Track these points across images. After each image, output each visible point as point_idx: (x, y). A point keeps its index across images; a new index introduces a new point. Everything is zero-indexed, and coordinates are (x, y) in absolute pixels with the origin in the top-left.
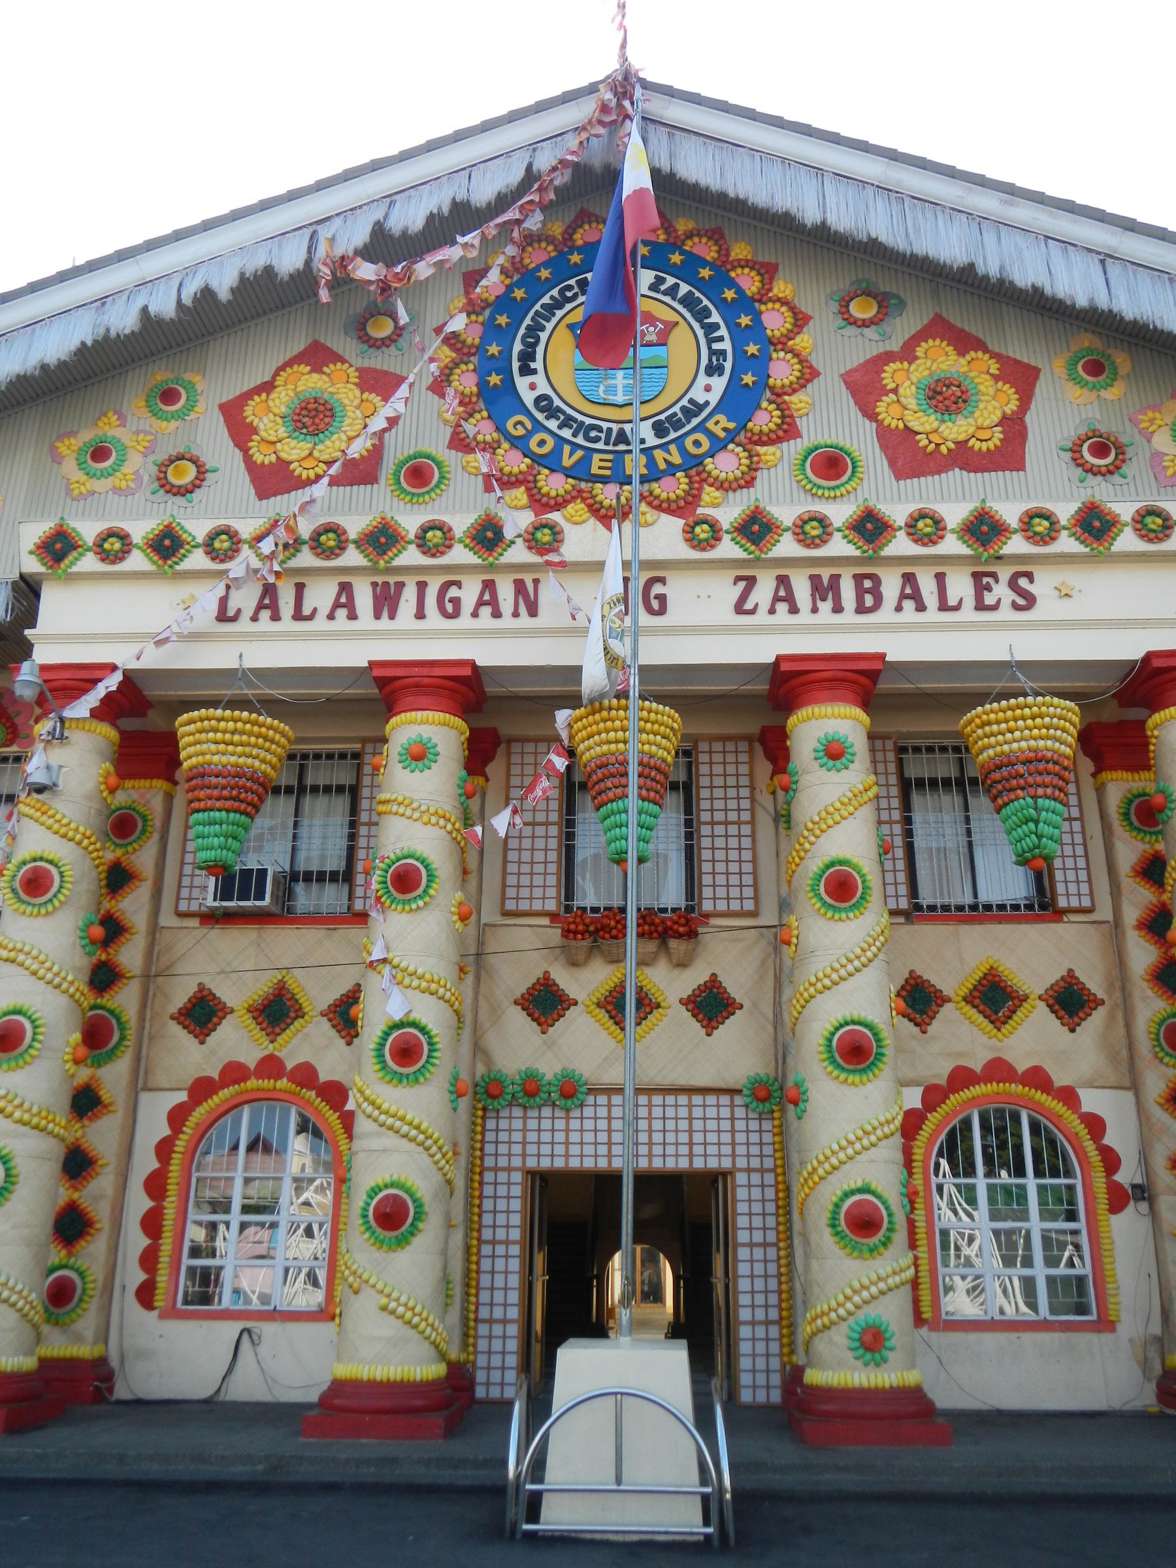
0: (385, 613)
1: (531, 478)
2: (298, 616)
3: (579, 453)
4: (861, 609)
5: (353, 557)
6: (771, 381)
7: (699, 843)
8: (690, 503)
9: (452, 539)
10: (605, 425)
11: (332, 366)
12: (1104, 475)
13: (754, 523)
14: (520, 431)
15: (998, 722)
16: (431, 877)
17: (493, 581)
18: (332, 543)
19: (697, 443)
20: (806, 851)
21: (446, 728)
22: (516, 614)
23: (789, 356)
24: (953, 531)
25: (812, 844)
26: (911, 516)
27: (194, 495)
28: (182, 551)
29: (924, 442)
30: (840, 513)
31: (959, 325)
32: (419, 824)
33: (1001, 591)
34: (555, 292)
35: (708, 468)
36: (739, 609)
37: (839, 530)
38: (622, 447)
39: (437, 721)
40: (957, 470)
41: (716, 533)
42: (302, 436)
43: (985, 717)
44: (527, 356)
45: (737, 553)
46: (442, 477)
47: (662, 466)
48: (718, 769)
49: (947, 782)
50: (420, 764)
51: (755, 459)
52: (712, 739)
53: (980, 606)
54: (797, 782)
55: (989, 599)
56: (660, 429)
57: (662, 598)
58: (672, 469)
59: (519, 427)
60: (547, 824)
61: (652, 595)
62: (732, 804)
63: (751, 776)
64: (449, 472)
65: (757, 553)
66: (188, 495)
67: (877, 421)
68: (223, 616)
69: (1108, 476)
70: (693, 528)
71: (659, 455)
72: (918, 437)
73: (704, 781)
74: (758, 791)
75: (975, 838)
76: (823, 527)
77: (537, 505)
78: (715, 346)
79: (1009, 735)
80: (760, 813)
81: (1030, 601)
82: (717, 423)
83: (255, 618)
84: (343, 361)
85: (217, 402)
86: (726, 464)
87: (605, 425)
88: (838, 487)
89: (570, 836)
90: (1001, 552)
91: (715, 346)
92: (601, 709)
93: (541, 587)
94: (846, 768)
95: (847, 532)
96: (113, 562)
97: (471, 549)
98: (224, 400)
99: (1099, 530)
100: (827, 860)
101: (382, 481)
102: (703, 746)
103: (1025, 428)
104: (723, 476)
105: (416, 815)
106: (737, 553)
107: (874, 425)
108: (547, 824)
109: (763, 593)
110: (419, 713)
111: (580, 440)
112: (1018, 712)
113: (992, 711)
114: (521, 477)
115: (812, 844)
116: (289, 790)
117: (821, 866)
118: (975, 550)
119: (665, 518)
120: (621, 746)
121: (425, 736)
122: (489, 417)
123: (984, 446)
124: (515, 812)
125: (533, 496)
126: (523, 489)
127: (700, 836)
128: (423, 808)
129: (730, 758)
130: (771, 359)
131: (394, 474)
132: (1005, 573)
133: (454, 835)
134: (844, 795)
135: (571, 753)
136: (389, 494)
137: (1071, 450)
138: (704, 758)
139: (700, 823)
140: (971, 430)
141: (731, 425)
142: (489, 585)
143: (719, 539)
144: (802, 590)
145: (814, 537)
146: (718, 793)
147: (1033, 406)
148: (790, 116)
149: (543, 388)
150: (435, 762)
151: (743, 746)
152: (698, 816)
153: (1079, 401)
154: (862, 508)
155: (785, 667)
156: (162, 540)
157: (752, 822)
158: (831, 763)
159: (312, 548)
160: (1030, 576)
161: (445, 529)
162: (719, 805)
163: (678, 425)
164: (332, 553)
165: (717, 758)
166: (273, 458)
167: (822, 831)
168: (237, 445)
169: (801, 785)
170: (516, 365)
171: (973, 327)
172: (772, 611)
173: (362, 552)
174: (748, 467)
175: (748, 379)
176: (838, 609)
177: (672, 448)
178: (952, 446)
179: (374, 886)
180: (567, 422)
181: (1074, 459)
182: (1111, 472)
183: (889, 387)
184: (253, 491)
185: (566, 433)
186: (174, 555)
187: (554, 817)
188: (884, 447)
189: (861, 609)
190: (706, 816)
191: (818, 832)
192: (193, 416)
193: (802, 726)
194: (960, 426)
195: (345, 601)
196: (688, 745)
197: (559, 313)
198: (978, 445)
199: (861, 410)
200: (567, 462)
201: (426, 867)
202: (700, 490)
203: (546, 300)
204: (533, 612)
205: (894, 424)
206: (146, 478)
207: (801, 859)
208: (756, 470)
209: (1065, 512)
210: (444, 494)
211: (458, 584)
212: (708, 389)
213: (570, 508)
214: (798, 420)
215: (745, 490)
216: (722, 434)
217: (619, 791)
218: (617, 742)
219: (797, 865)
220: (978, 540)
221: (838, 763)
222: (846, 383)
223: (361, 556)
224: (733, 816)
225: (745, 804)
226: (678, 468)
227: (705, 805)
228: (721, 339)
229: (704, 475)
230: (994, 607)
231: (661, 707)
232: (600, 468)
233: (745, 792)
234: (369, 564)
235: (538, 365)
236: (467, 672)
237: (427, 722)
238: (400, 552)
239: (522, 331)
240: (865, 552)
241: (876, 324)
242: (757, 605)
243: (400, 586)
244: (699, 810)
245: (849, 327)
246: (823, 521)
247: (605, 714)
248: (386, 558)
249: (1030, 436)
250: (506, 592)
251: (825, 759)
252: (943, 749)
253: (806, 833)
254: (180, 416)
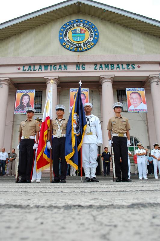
10: (76, 44)
14: (65, 45)
19: (89, 46)
34: (69, 26)
38: (79, 47)
44: (65, 35)
47: (84, 49)
56: (84, 45)
57: (84, 67)
71: (84, 48)
78: (92, 34)
83: (28, 71)
87: (76, 44)
91: (92, 34)
111: (73, 46)
141: (94, 44)
163: (86, 44)
170: (64, 36)
175: (96, 38)
180: (71, 44)
185: (71, 45)
197: (70, 29)
200: (71, 49)
203: (68, 27)
212: (91, 39)
228: (92, 33)
230: (129, 69)
235: (67, 36)
239: (65, 31)
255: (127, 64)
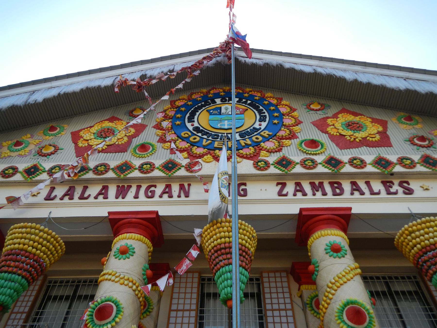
0: (121, 197)
1: (190, 149)
2: (82, 197)
3: (210, 141)
4: (335, 194)
5: (111, 174)
6: (284, 123)
7: (266, 320)
8: (255, 156)
9: (154, 168)
11: (117, 121)
12: (426, 147)
13: (284, 161)
14: (186, 135)
15: (419, 230)
16: (119, 311)
17: (170, 185)
18: (103, 169)
19: (257, 138)
20: (331, 299)
21: (141, 243)
22: (179, 196)
23: (290, 117)
24: (370, 164)
25: (333, 295)
26: (350, 159)
27: (50, 156)
28: (38, 173)
29: (349, 138)
30: (319, 159)
31: (352, 111)
32: (118, 284)
33: (395, 187)
35: (262, 145)
36: (280, 194)
37: (320, 164)
39: (136, 238)
40: (365, 147)
41: (267, 165)
42: (100, 138)
43: (410, 229)
45: (277, 171)
46: (153, 149)
47: (243, 144)
48: (273, 285)
49: (384, 293)
50: (124, 256)
51: (281, 143)
52: (269, 271)
53: (389, 193)
54: (318, 266)
55: (392, 190)
57: (245, 191)
58: (247, 146)
59: (186, 134)
60: (190, 310)
61: (240, 189)
62: (282, 301)
63: (289, 287)
64: (156, 148)
65: (286, 170)
66: (48, 156)
67: (328, 133)
68: (48, 198)
69: (429, 148)
70: (257, 163)
72: (346, 137)
73: (267, 290)
74: (293, 296)
75: (405, 319)
76: (313, 163)
77: (192, 157)
79: (426, 236)
80: (295, 306)
81: (409, 191)
82: (265, 133)
84: (121, 120)
85: (71, 131)
86: (270, 145)
88: (317, 151)
89: (202, 318)
90: (393, 171)
92: (217, 223)
93: (191, 187)
94: (344, 257)
95: (324, 164)
96: (7, 177)
97: (162, 171)
98: (74, 131)
99: (433, 163)
100: (344, 301)
101: (129, 151)
102: (265, 275)
103: (388, 135)
104: (268, 148)
105: (117, 279)
106: (277, 171)
107: (327, 135)
108: (190, 310)
109: (290, 188)
110: (128, 234)
112: (428, 224)
113: (413, 225)
114: (186, 149)
115: (333, 295)
116: (67, 298)
117: (341, 305)
118: (381, 170)
119: (245, 161)
120: (227, 239)
121: (129, 244)
122: (175, 133)
123: (374, 139)
124: (169, 277)
125: (189, 154)
126: (186, 152)
127: (266, 317)
128: (122, 276)
129: (278, 279)
130: (283, 118)
131: (134, 149)
132: (396, 182)
133: (137, 292)
134: (345, 269)
135: (201, 249)
136: (131, 154)
137: (410, 141)
138: (265, 280)
139: (266, 310)
140: (367, 135)
141: (270, 133)
142: (168, 186)
143: (269, 167)
144: (307, 188)
145: (310, 166)
146: (274, 295)
147: (388, 130)
148: (284, 51)
149: (196, 124)
150: (133, 256)
151: (284, 274)
152: (265, 307)
153: (406, 128)
154: (328, 156)
155: (304, 213)
156: (31, 169)
157: (292, 309)
158: (335, 254)
159: (94, 171)
160: (408, 183)
161: (151, 164)
162: (275, 301)
164: (102, 173)
165: (272, 280)
166: (86, 145)
167: (338, 287)
168: (74, 142)
169: (321, 267)
171: (358, 111)
172: (295, 195)
173: (114, 172)
174: (279, 145)
176: (325, 194)
177: (248, 140)
178: (361, 139)
179: (86, 317)
180: (206, 134)
181: (412, 143)
182: (429, 147)
183: (330, 124)
184: (75, 155)
186: (34, 174)
187: (194, 307)
188: (333, 140)
189: (335, 194)
190: (269, 307)
191: (335, 288)
192: (60, 135)
193: (317, 241)
194: (362, 134)
195: (104, 192)
196: (257, 276)
198: (371, 139)
199: (321, 131)
201: (117, 306)
202: (259, 152)
204: (187, 196)
205: (335, 134)
206: (33, 152)
207: (328, 304)
208: (282, 146)
209: (416, 158)
210: (153, 155)
211: (155, 186)
213: (205, 157)
214: (296, 134)
215: (278, 153)
216: (267, 136)
217: (226, 262)
218: (225, 237)
219: (326, 309)
220: (381, 166)
221: (339, 254)
222: (313, 124)
223: (114, 174)
224: (282, 306)
225: (288, 301)
226: (250, 145)
227: (268, 301)
229: (261, 148)
231: (247, 224)
232: (218, 145)
233: (287, 295)
234: (117, 176)
236: (154, 216)
237: (131, 238)
238: (131, 172)
239: (190, 111)
240: (333, 170)
241: (321, 110)
242: (288, 192)
243: (130, 187)
244: (265, 304)
245: (311, 111)
246: (313, 161)
247: (219, 225)
248: (124, 174)
249: (391, 137)
250: (175, 188)
251: (332, 253)
252: (378, 278)
253: (328, 290)
254: (55, 135)
255: (383, 182)
